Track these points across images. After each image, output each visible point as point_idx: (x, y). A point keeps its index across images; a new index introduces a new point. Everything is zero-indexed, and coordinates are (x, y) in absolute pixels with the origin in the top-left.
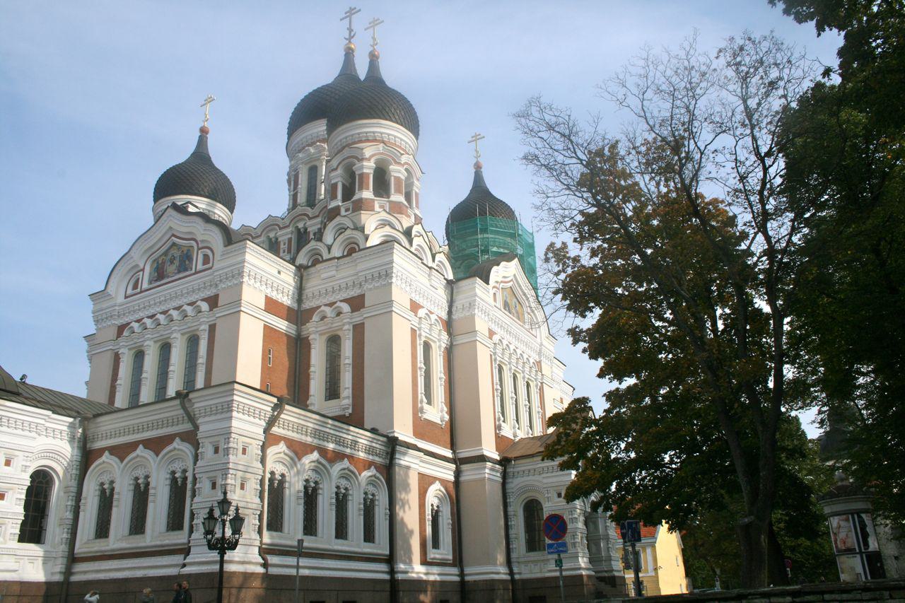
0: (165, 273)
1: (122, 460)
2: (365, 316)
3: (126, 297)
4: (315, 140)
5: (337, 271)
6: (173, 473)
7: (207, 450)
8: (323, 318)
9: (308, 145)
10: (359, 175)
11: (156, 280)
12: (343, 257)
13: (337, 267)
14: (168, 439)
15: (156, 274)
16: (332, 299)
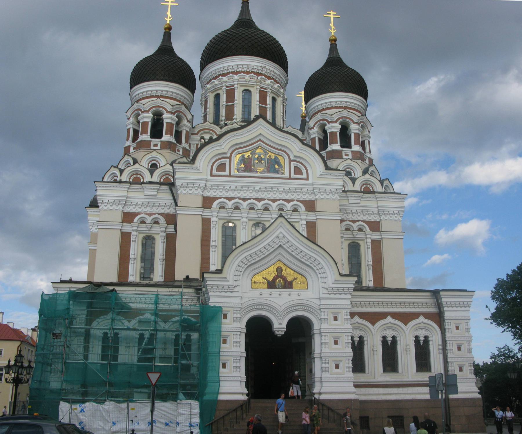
0: (253, 167)
1: (373, 324)
2: (383, 237)
3: (212, 175)
4: (250, 70)
5: (361, 200)
6: (417, 337)
7: (450, 325)
8: (347, 229)
9: (244, 72)
10: (355, 134)
11: (244, 171)
12: (360, 192)
13: (361, 197)
14: (416, 316)
15: (242, 166)
16: (355, 218)
